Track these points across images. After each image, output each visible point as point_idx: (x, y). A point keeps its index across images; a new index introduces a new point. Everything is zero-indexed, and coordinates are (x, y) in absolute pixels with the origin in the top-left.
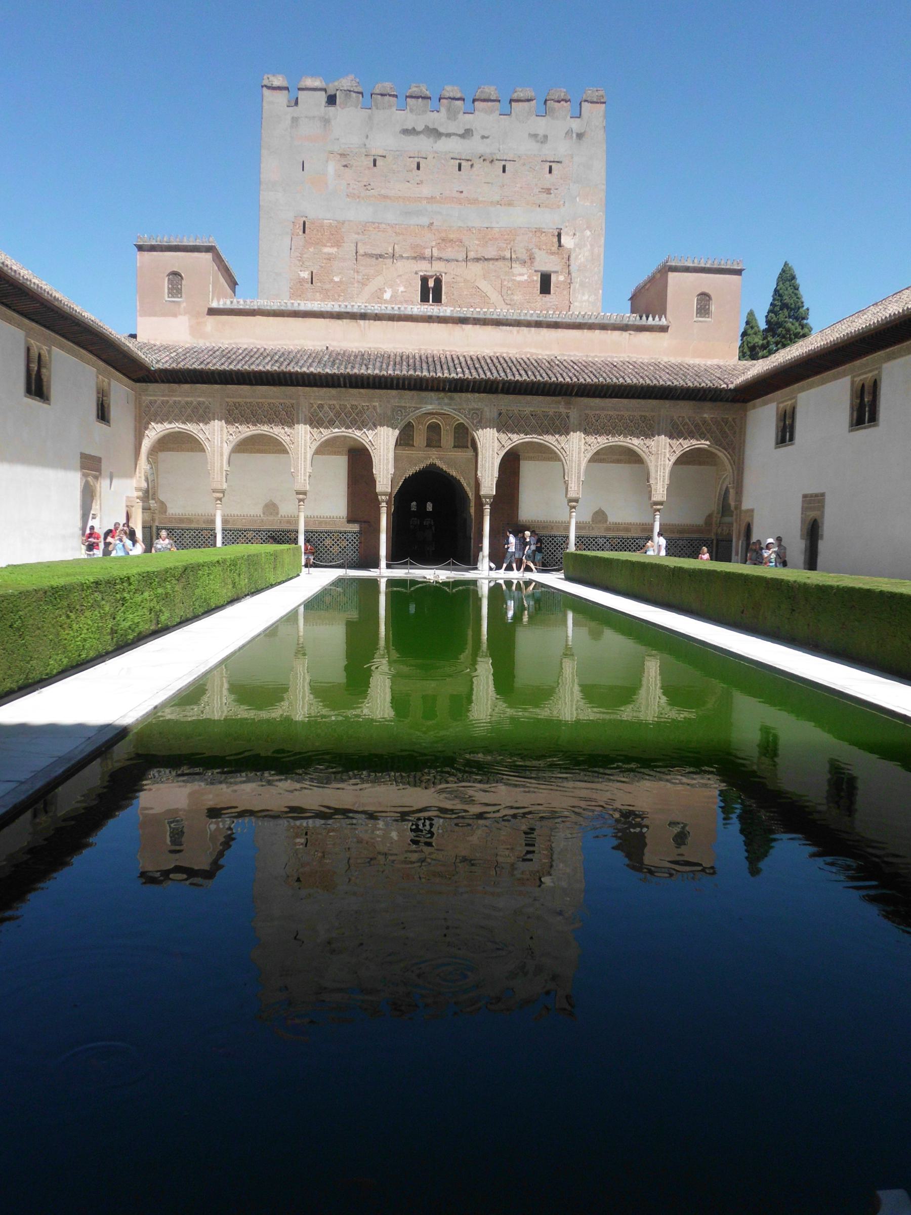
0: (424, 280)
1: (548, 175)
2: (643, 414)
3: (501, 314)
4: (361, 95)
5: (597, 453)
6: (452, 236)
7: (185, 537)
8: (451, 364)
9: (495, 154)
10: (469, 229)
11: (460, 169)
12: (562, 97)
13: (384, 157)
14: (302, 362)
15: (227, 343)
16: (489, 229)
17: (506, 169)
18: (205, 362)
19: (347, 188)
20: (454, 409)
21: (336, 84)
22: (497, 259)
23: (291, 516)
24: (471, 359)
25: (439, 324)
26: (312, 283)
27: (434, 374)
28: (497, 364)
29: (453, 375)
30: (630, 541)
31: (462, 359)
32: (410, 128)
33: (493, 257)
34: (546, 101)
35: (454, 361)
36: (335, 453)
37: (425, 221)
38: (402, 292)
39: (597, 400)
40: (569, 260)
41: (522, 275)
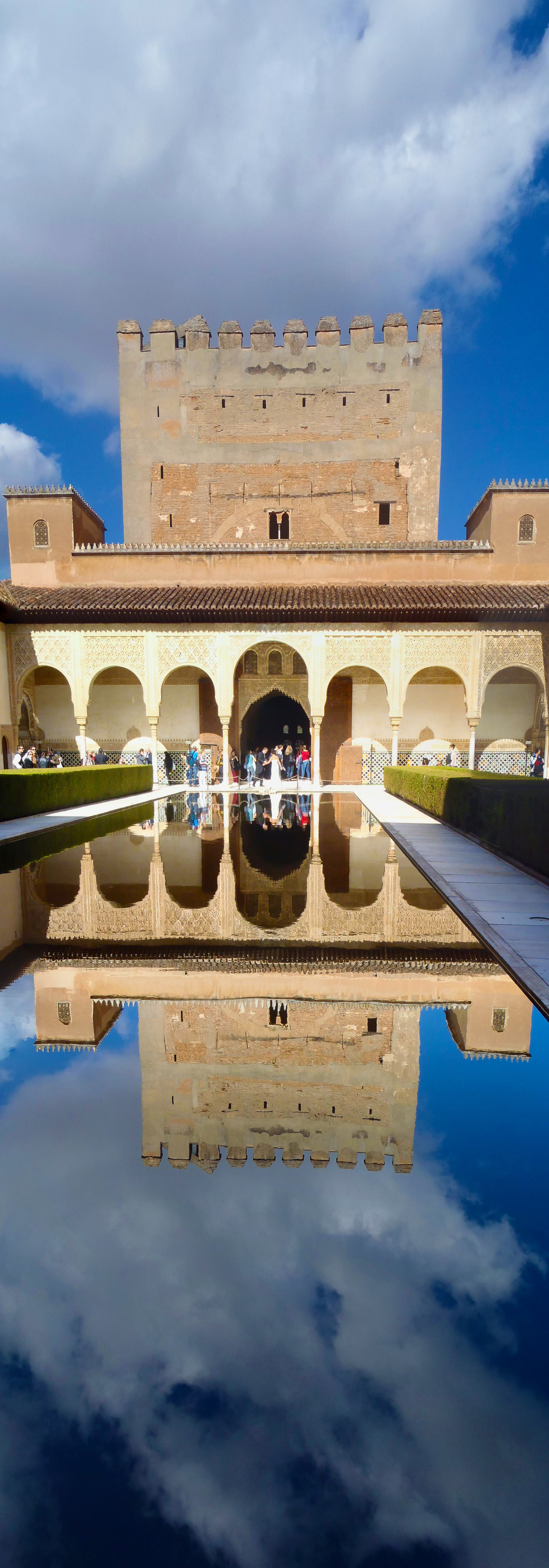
0: (273, 516)
1: (386, 405)
4: (208, 334)
8: (284, 597)
11: (304, 405)
12: (400, 322)
13: (233, 397)
18: (64, 603)
19: (199, 431)
21: (185, 325)
22: (339, 493)
31: (297, 592)
32: (255, 367)
33: (335, 491)
37: (271, 459)
40: (406, 489)
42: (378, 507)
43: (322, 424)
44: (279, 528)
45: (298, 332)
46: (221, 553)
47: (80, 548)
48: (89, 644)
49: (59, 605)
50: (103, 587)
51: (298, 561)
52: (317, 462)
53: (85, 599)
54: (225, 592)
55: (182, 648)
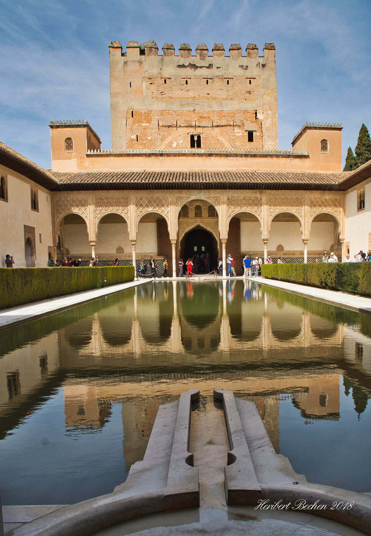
0: (192, 137)
3: (228, 151)
6: (205, 115)
8: (204, 176)
11: (207, 83)
13: (170, 78)
14: (131, 178)
15: (96, 171)
16: (222, 111)
17: (229, 82)
18: (84, 180)
20: (206, 198)
24: (214, 174)
25: (199, 158)
27: (195, 181)
29: (204, 181)
30: (295, 260)
31: (209, 173)
32: (182, 64)
33: (225, 125)
34: (246, 49)
35: (206, 174)
37: (191, 109)
42: (247, 133)
43: (217, 93)
44: (196, 142)
45: (203, 50)
46: (168, 154)
48: (98, 201)
49: (82, 181)
50: (104, 172)
51: (209, 158)
52: (214, 111)
53: (95, 178)
54: (171, 174)
55: (149, 203)
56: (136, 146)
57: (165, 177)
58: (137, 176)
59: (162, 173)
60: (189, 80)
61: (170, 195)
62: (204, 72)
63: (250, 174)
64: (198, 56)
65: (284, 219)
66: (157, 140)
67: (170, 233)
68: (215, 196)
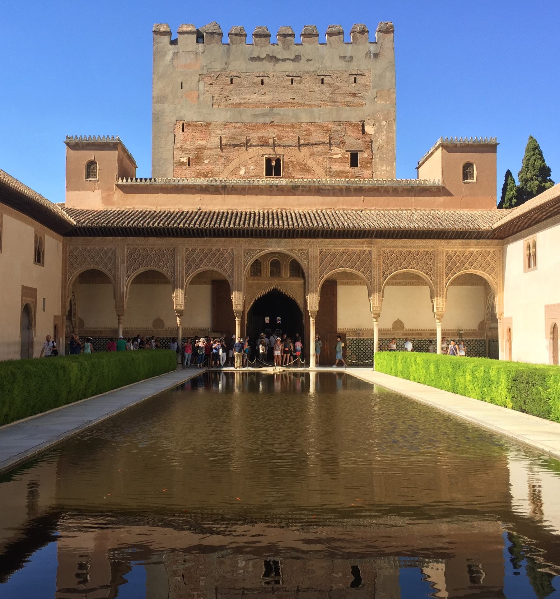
0: (269, 161)
1: (354, 84)
2: (426, 250)
5: (393, 278)
7: (97, 344)
8: (285, 219)
9: (316, 71)
10: (300, 124)
11: (292, 83)
13: (238, 77)
20: (288, 250)
22: (320, 144)
23: (173, 329)
26: (189, 165)
28: (318, 219)
29: (286, 227)
30: (422, 343)
31: (293, 215)
36: (205, 283)
37: (268, 120)
38: (252, 169)
39: (391, 241)
41: (337, 154)
47: (122, 181)
50: (140, 211)
56: (187, 173)
57: (228, 220)
58: (189, 218)
59: (223, 213)
60: (265, 79)
61: (235, 246)
62: (289, 67)
63: (354, 217)
64: (279, 43)
65: (405, 282)
66: (218, 165)
67: (233, 301)
68: (300, 248)
